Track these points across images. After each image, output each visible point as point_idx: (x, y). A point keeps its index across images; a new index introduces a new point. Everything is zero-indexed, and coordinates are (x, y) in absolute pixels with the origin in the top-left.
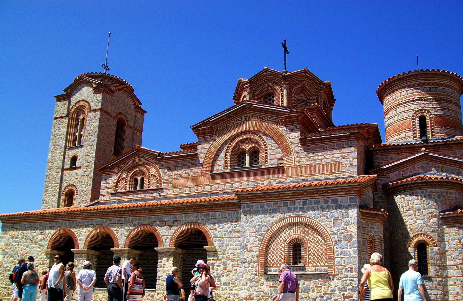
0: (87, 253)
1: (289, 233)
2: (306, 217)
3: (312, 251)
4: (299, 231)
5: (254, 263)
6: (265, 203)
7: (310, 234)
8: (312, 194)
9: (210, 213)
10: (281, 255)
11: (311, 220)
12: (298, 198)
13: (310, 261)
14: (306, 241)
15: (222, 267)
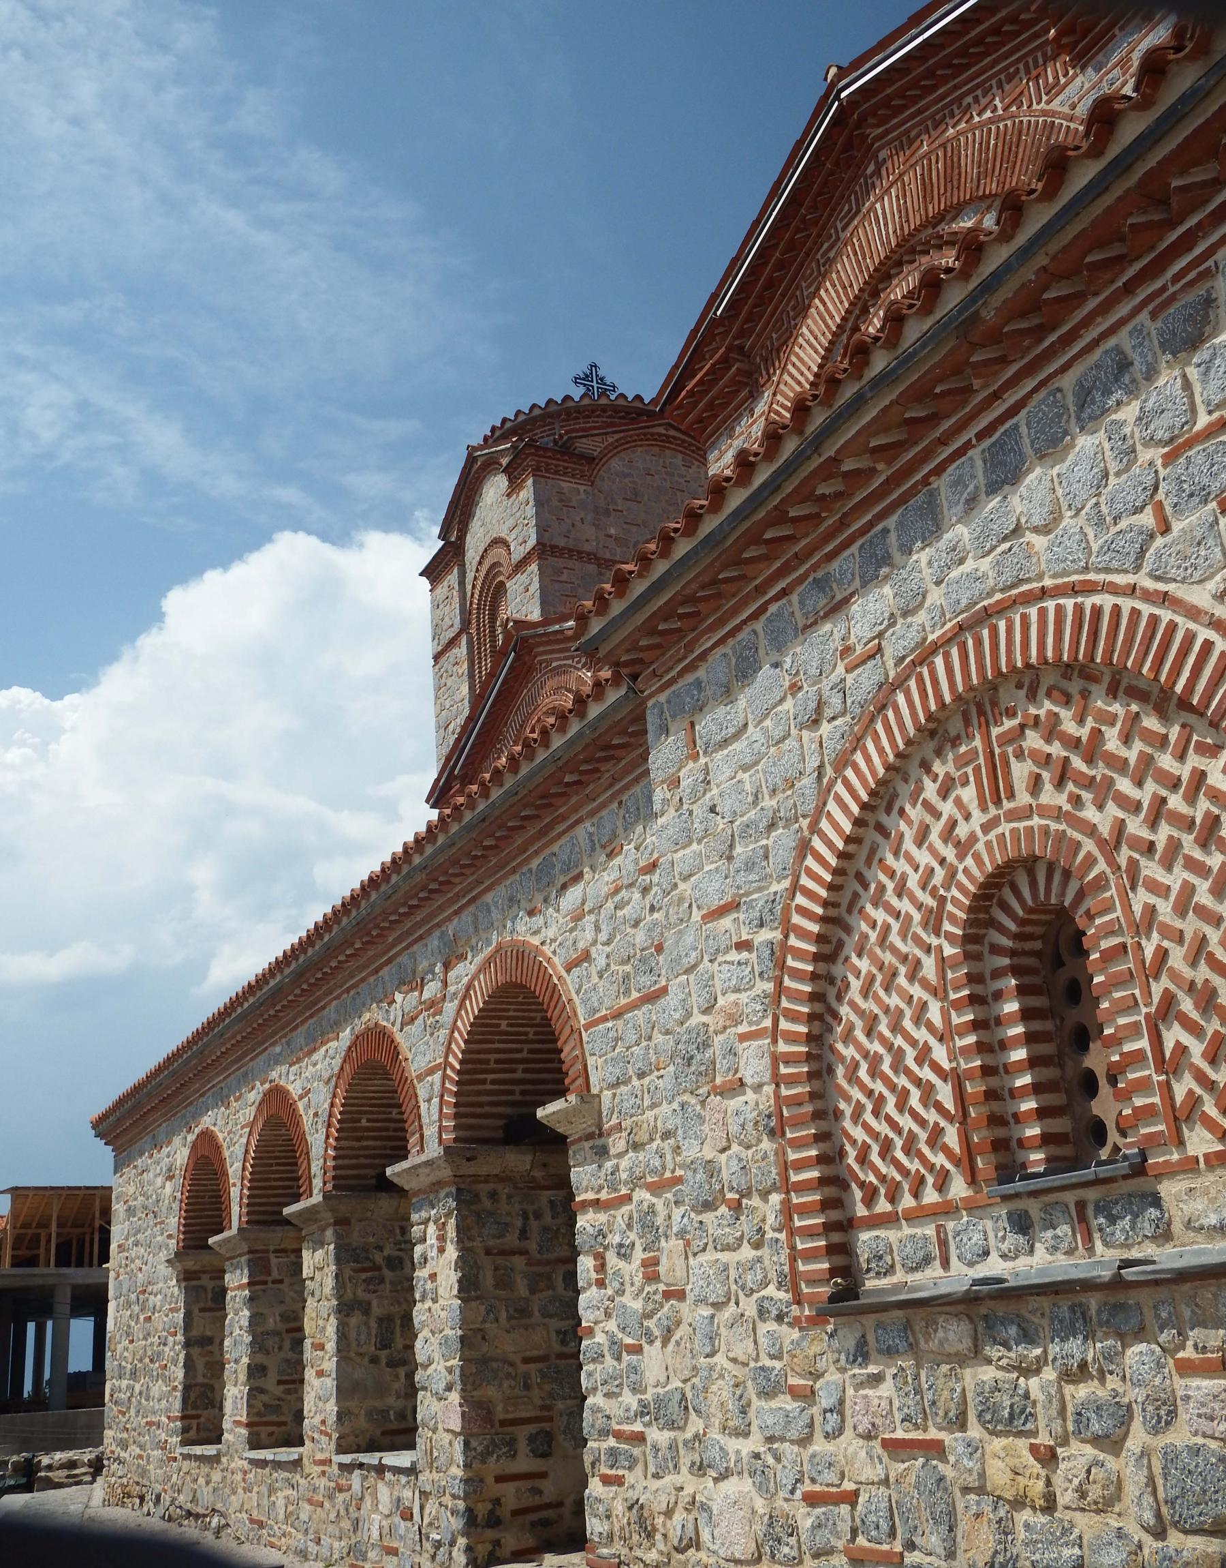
0: (250, 1252)
1: (953, 824)
2: (1044, 593)
3: (1177, 958)
4: (1020, 771)
5: (764, 1195)
6: (758, 626)
7: (1120, 765)
8: (1041, 331)
9: (555, 848)
10: (926, 1074)
11: (1089, 602)
12: (943, 441)
13: (1180, 1091)
14: (1102, 866)
15: (639, 1255)
